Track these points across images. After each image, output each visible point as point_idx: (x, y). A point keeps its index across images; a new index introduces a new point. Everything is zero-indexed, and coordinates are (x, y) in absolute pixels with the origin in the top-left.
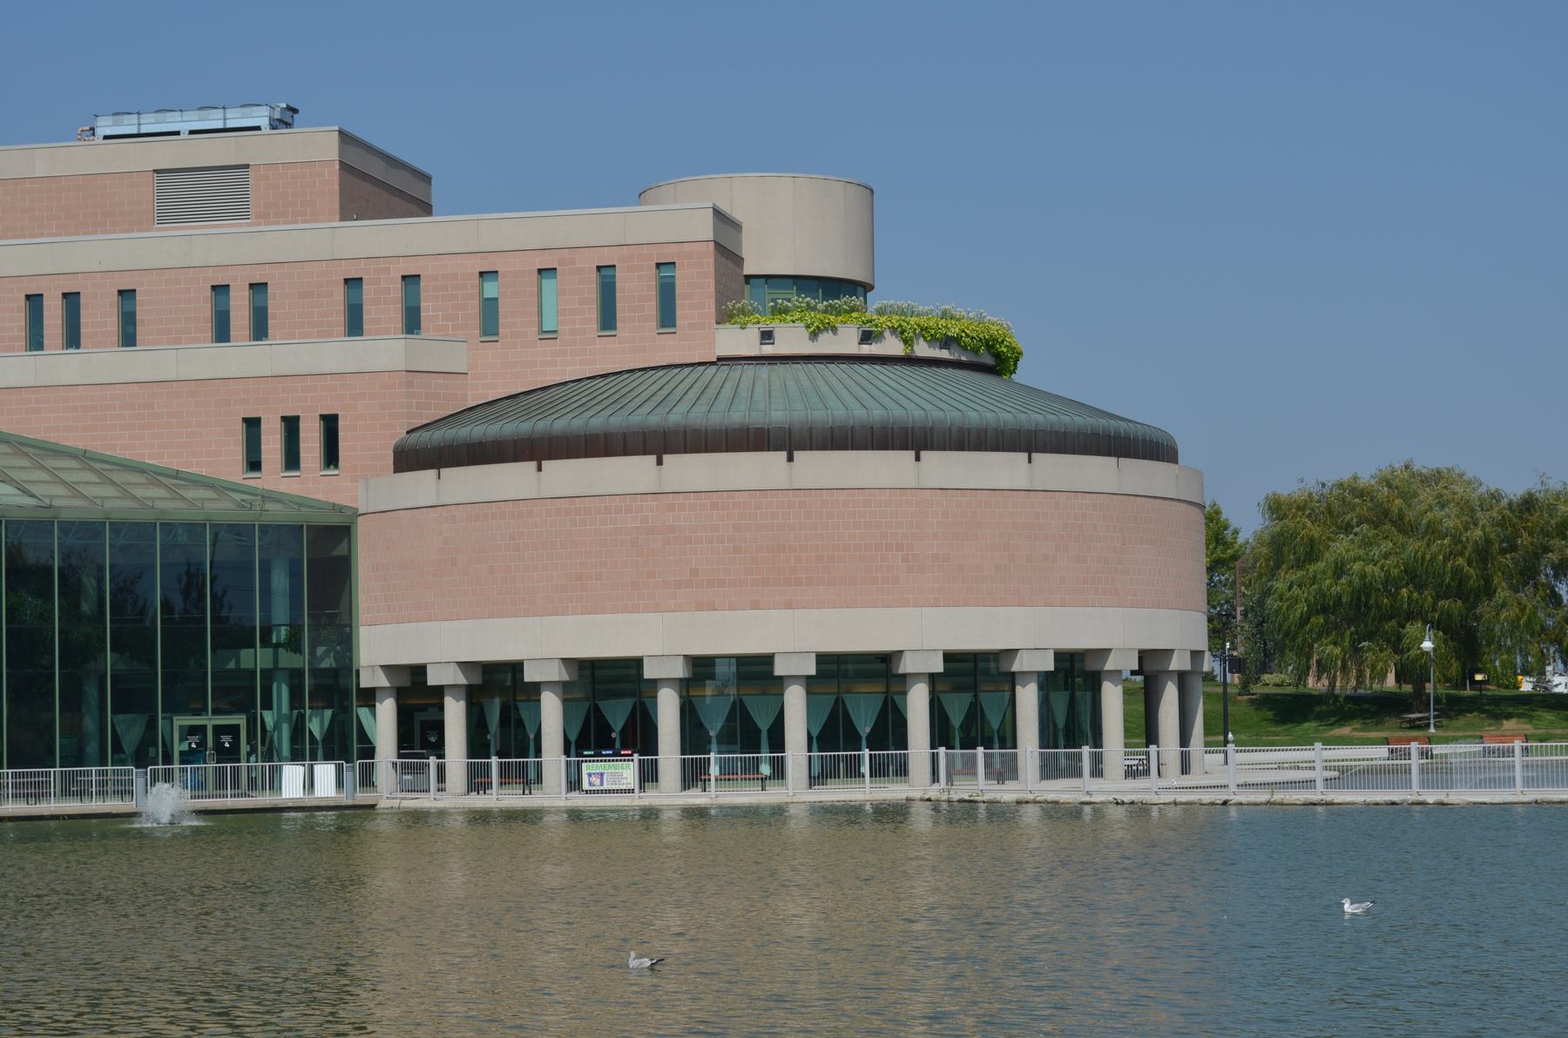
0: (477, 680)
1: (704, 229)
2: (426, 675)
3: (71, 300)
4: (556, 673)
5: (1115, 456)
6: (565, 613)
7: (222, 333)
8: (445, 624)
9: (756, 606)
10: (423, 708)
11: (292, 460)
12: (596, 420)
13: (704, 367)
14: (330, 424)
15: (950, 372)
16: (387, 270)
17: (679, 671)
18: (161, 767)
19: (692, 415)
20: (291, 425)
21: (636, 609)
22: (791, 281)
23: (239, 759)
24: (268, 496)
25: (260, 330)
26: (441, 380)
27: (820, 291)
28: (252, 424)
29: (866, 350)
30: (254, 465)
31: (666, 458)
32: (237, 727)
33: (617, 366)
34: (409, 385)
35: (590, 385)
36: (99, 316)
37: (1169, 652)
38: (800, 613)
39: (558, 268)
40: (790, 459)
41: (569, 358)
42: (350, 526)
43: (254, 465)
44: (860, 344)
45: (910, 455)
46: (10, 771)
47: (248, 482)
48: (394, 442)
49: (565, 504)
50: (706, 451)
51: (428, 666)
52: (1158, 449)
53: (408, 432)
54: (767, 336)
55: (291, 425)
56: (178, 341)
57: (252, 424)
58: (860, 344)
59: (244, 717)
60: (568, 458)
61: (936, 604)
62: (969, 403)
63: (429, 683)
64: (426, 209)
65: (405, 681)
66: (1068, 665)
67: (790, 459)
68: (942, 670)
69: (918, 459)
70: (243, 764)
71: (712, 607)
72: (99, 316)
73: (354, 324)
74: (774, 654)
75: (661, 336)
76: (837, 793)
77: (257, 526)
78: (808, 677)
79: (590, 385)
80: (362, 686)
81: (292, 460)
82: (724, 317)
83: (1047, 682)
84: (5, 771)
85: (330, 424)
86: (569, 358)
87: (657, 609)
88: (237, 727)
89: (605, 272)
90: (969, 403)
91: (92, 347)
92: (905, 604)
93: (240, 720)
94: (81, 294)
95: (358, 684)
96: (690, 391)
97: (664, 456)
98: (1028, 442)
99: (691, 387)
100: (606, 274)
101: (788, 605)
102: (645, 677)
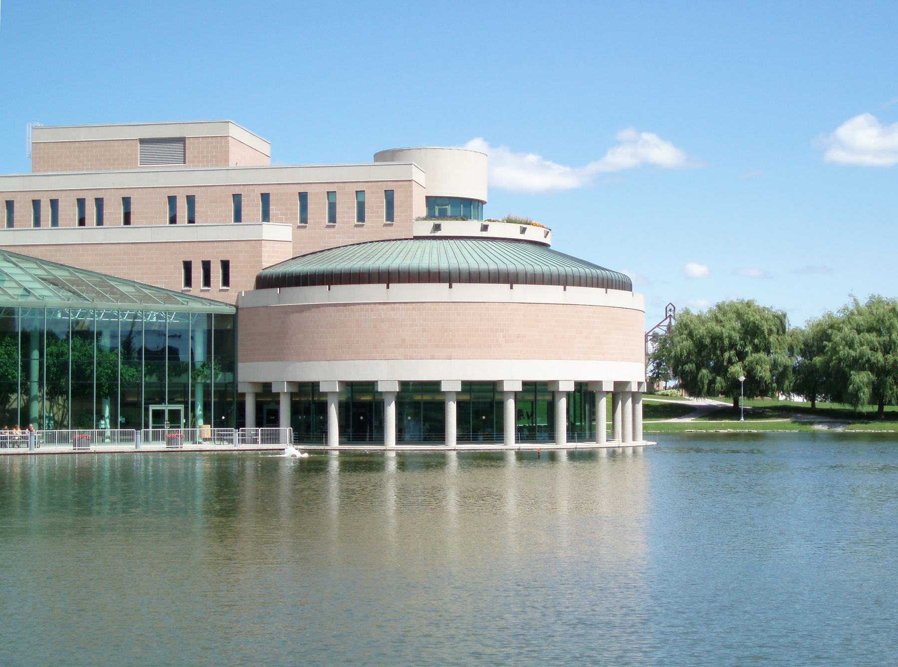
0: (295, 390)
3: (99, 203)
10: (268, 403)
11: (207, 282)
13: (407, 241)
14: (225, 265)
16: (254, 191)
18: (119, 430)
20: (206, 265)
22: (448, 199)
23: (180, 426)
27: (462, 205)
28: (188, 266)
30: (188, 282)
31: (391, 285)
32: (179, 411)
33: (364, 239)
35: (351, 249)
36: (114, 211)
40: (450, 287)
41: (341, 235)
43: (188, 282)
46: (97, 430)
48: (257, 274)
54: (437, 228)
55: (206, 265)
57: (188, 266)
59: (183, 406)
62: (536, 262)
63: (273, 391)
66: (579, 388)
67: (450, 287)
68: (521, 390)
69: (511, 288)
70: (182, 429)
72: (114, 211)
73: (238, 218)
79: (351, 249)
80: (239, 392)
81: (207, 282)
84: (95, 430)
85: (225, 265)
86: (341, 235)
88: (180, 410)
89: (360, 195)
90: (536, 262)
91: (109, 225)
93: (181, 407)
95: (237, 391)
96: (401, 253)
98: (564, 281)
99: (401, 251)
101: (449, 358)
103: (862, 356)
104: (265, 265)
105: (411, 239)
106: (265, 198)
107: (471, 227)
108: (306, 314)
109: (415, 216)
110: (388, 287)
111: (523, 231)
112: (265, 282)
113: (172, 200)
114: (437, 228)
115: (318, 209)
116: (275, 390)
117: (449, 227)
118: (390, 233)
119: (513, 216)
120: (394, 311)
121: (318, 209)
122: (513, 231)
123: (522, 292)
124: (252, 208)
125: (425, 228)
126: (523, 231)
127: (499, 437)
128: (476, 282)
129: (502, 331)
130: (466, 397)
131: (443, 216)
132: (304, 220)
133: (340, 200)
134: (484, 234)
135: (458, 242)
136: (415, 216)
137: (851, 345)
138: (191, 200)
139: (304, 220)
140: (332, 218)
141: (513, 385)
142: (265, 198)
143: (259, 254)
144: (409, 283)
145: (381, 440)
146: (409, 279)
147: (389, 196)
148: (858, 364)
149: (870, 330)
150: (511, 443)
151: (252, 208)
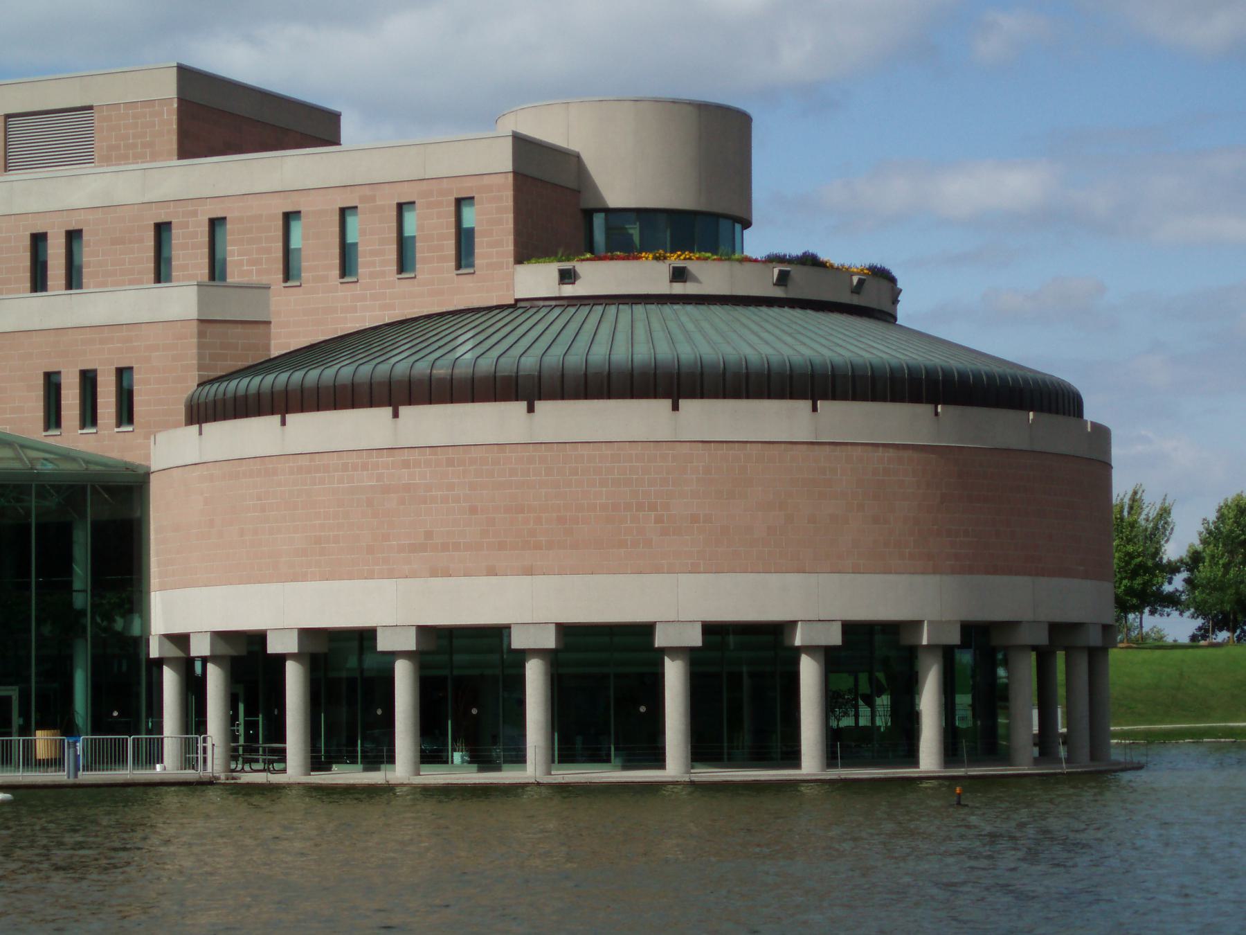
1: (502, 160)
2: (376, 639)
4: (410, 643)
5: (928, 401)
6: (303, 578)
7: (39, 282)
8: (205, 590)
9: (492, 572)
11: (89, 416)
12: (342, 370)
15: (775, 312)
17: (549, 641)
19: (547, 359)
20: (88, 380)
21: (370, 576)
24: (67, 456)
25: (73, 279)
26: (239, 329)
29: (679, 289)
33: (416, 310)
34: (201, 334)
37: (793, 624)
38: (539, 580)
39: (359, 206)
40: (531, 409)
42: (142, 486)
44: (671, 281)
45: (666, 404)
47: (51, 441)
49: (304, 461)
50: (748, 397)
51: (191, 634)
53: (199, 385)
55: (88, 380)
56: (104, 284)
58: (671, 281)
60: (225, 419)
61: (694, 570)
64: (331, 138)
65: (240, 651)
67: (531, 409)
71: (447, 574)
73: (161, 272)
74: (656, 622)
75: (460, 277)
76: (435, 776)
77: (33, 486)
78: (692, 650)
81: (89, 416)
82: (521, 257)
83: (831, 659)
87: (390, 575)
92: (658, 570)
94: (173, 226)
97: (287, 415)
102: (656, 645)
105: (509, 306)
110: (283, 423)
113: (38, 240)
116: (275, 646)
120: (368, 470)
128: (716, 396)
129: (653, 507)
131: (587, 248)
135: (689, 308)
138: (73, 236)
144: (302, 411)
146: (353, 401)
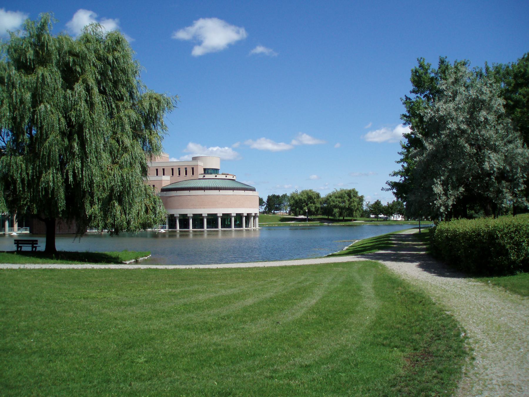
52: (254, 190)
54: (204, 176)
98: (233, 189)
100: (186, 168)
103: (336, 204)
104: (163, 186)
106: (164, 169)
107: (213, 176)
108: (171, 198)
109: (199, 173)
111: (226, 177)
112: (163, 190)
114: (204, 176)
115: (176, 172)
117: (207, 176)
118: (193, 178)
119: (224, 173)
121: (176, 172)
122: (224, 177)
123: (222, 192)
124: (160, 172)
125: (201, 177)
126: (226, 177)
127: (217, 227)
130: (181, 218)
132: (173, 175)
133: (181, 170)
134: (216, 178)
136: (199, 173)
137: (334, 202)
139: (173, 175)
140: (179, 174)
141: (220, 214)
142: (164, 169)
143: (161, 184)
145: (176, 228)
147: (193, 169)
148: (335, 207)
149: (339, 197)
150: (220, 228)
151: (160, 172)
